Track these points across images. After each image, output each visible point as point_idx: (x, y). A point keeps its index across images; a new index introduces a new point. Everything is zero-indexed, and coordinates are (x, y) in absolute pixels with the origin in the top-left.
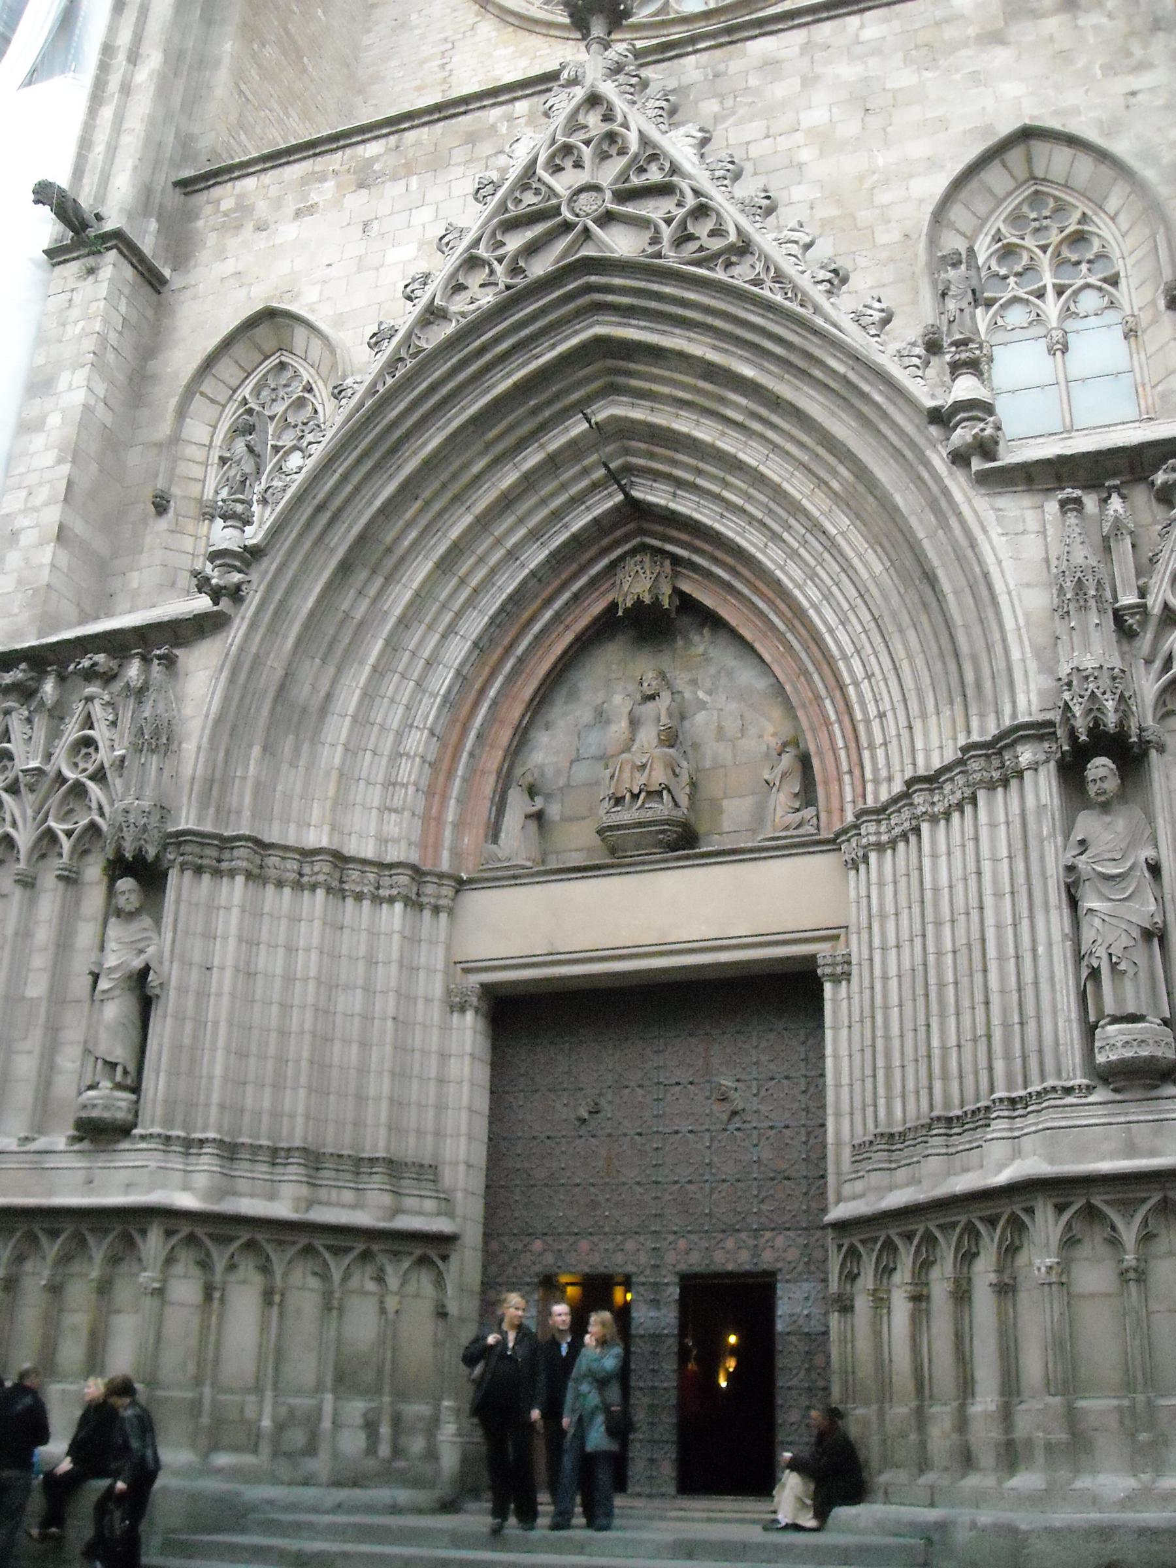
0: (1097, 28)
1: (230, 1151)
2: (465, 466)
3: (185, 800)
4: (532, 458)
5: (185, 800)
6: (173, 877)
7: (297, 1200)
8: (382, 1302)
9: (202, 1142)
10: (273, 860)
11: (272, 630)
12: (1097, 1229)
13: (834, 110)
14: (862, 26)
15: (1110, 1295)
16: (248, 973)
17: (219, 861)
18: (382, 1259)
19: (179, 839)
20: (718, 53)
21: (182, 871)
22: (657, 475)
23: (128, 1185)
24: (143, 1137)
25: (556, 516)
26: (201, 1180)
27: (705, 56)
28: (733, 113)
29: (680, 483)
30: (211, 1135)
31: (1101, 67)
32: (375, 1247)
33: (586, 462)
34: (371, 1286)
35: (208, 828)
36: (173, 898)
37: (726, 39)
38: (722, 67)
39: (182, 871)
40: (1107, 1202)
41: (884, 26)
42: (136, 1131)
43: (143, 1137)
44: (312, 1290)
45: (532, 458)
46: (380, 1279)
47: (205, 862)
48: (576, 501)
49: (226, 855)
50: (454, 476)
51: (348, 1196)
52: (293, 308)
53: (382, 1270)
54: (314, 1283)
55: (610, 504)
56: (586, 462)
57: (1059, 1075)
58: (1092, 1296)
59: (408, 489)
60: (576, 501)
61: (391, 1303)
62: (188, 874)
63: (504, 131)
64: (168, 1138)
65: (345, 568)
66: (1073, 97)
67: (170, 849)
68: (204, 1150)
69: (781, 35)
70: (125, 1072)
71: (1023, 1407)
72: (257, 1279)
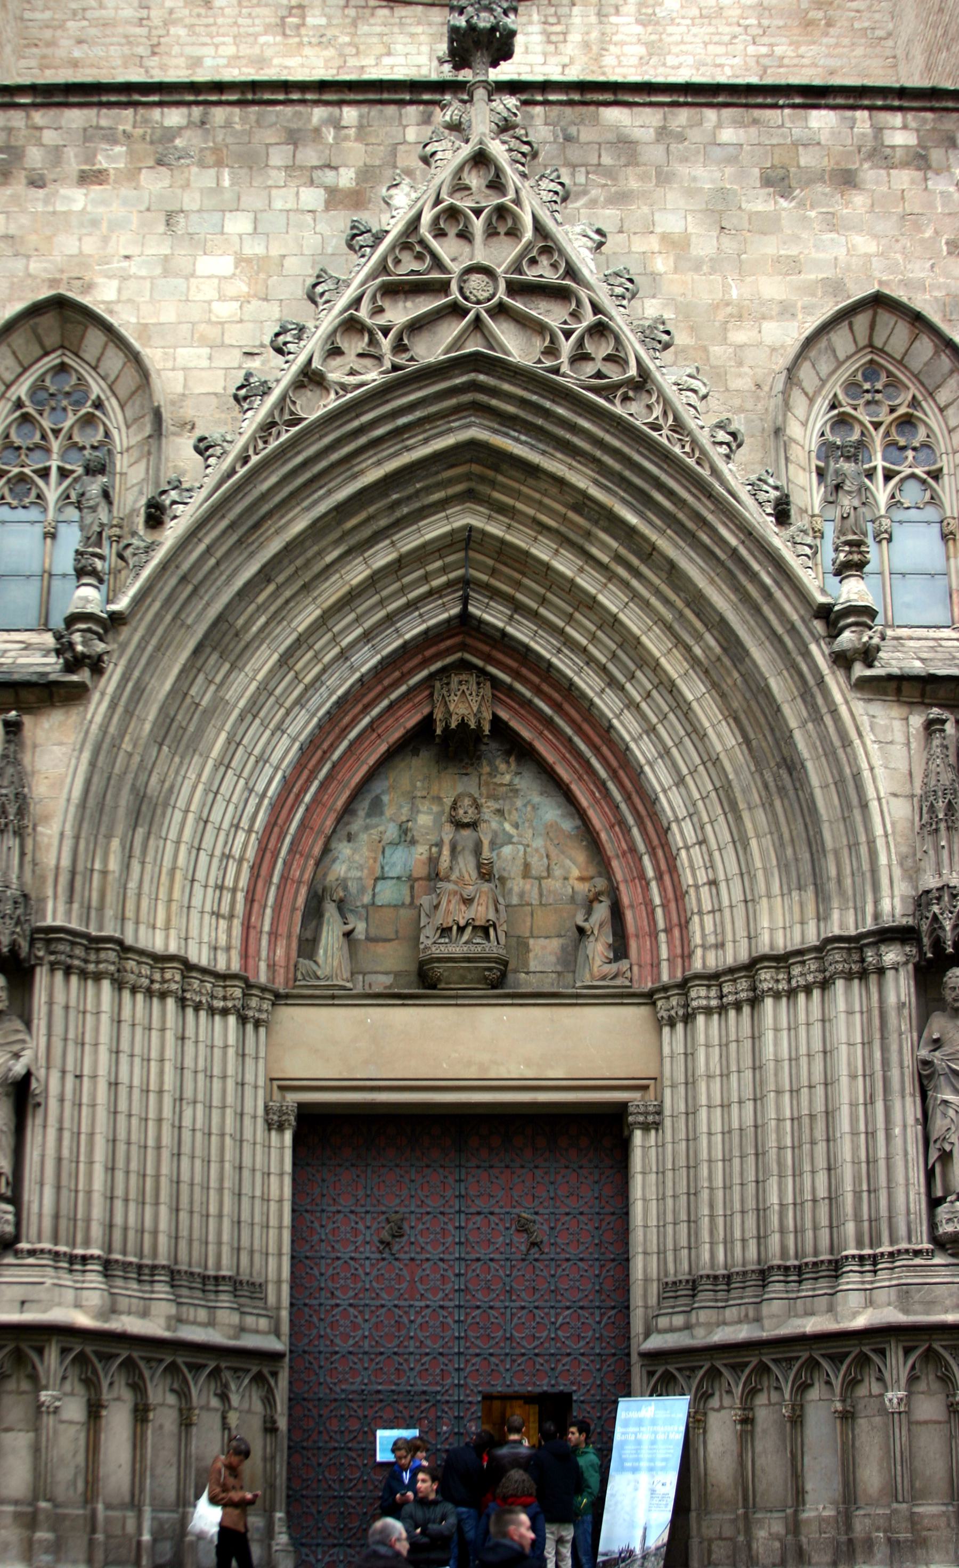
0: (944, 194)
1: (108, 1267)
2: (320, 554)
3: (50, 892)
4: (382, 556)
5: (50, 892)
6: (41, 977)
7: (169, 1318)
8: (224, 1418)
9: (85, 1259)
10: (131, 964)
11: (129, 713)
12: (931, 1368)
13: (689, 218)
14: (719, 125)
15: (939, 1422)
16: (114, 1085)
17: (86, 961)
18: (227, 1375)
19: (49, 935)
20: (568, 110)
21: (52, 970)
22: (494, 594)
23: (23, 1303)
24: (32, 1253)
25: (390, 619)
26: (94, 1299)
27: (556, 110)
28: (585, 193)
29: (518, 607)
30: (96, 1252)
31: (947, 243)
32: (223, 1365)
33: (430, 568)
34: (215, 1402)
35: (74, 925)
36: (44, 998)
37: (577, 97)
38: (573, 130)
39: (52, 970)
40: (944, 1347)
41: (741, 131)
42: (24, 1245)
43: (32, 1253)
44: (171, 1407)
45: (382, 556)
46: (224, 1397)
47: (76, 962)
48: (412, 605)
49: (93, 957)
50: (307, 564)
51: (202, 1314)
52: (86, 300)
53: (226, 1386)
54: (171, 1399)
55: (445, 616)
56: (430, 568)
57: (910, 1241)
58: (926, 1423)
59: (265, 575)
60: (412, 605)
61: (233, 1418)
62: (59, 975)
63: (331, 140)
64: (57, 1254)
65: (197, 651)
66: (919, 270)
67: (39, 945)
68: (89, 1267)
69: (636, 110)
70: (8, 1183)
71: (862, 1512)
72: (127, 1395)
